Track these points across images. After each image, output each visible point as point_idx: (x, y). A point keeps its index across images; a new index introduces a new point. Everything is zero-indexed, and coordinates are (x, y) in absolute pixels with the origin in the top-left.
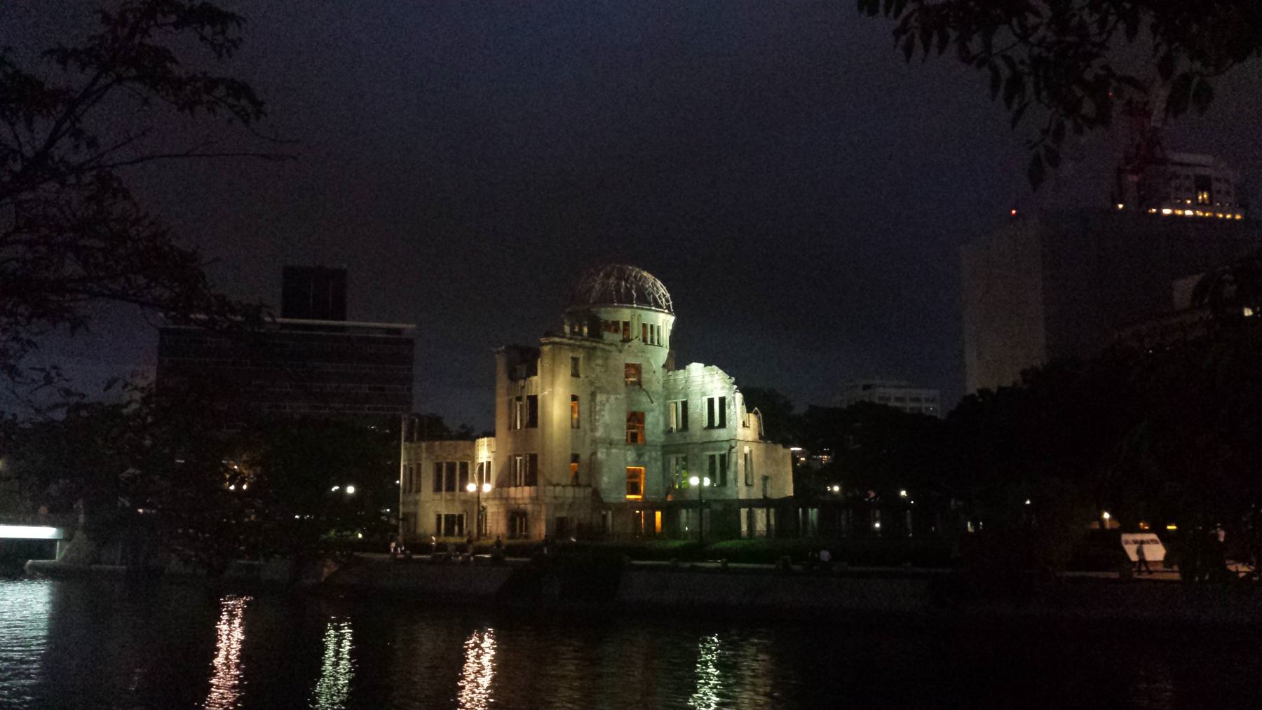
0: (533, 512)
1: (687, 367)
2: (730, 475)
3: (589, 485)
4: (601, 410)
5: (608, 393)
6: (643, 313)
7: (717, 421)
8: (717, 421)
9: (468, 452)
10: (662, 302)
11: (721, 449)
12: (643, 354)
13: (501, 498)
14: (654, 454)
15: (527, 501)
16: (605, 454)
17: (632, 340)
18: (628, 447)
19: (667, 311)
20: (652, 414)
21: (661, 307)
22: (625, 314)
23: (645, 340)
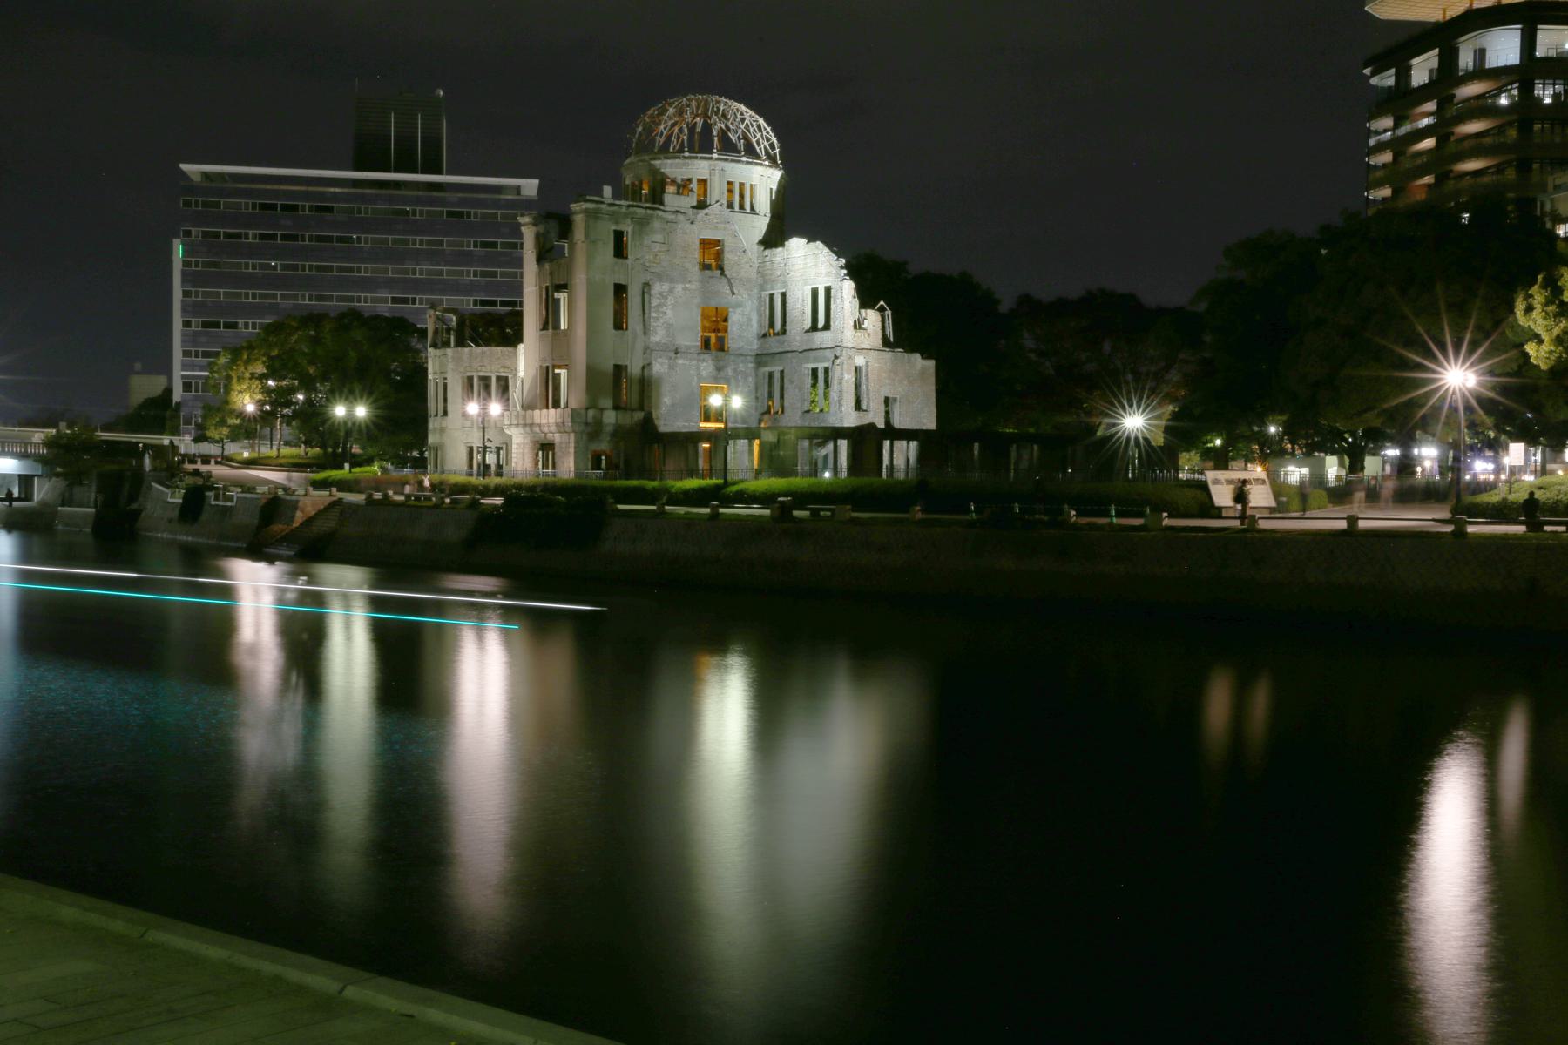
0: (561, 443)
1: (786, 243)
2: (834, 395)
3: (641, 408)
4: (659, 305)
5: (672, 280)
6: (728, 166)
7: (821, 323)
8: (821, 323)
9: (508, 363)
10: (761, 149)
11: (824, 359)
12: (728, 225)
13: (525, 425)
14: (741, 367)
15: (553, 428)
16: (666, 367)
17: (710, 205)
18: (702, 356)
19: (767, 163)
20: (739, 310)
21: (759, 157)
22: (700, 168)
23: (730, 205)
